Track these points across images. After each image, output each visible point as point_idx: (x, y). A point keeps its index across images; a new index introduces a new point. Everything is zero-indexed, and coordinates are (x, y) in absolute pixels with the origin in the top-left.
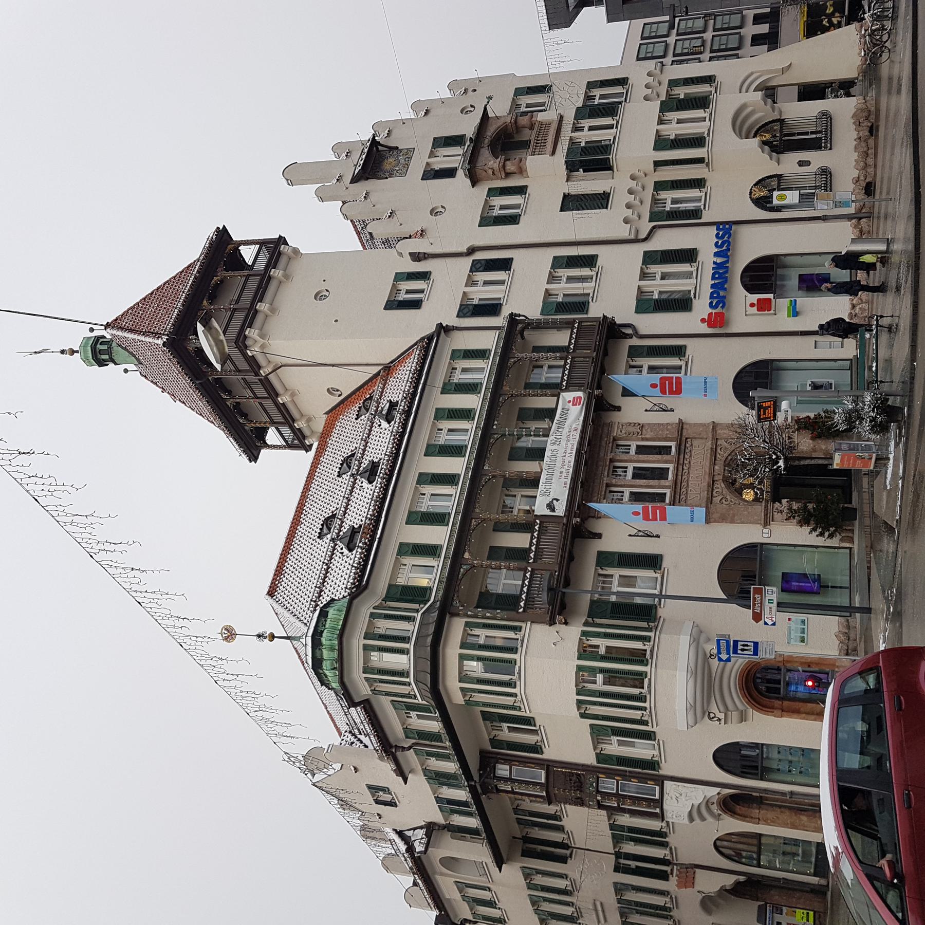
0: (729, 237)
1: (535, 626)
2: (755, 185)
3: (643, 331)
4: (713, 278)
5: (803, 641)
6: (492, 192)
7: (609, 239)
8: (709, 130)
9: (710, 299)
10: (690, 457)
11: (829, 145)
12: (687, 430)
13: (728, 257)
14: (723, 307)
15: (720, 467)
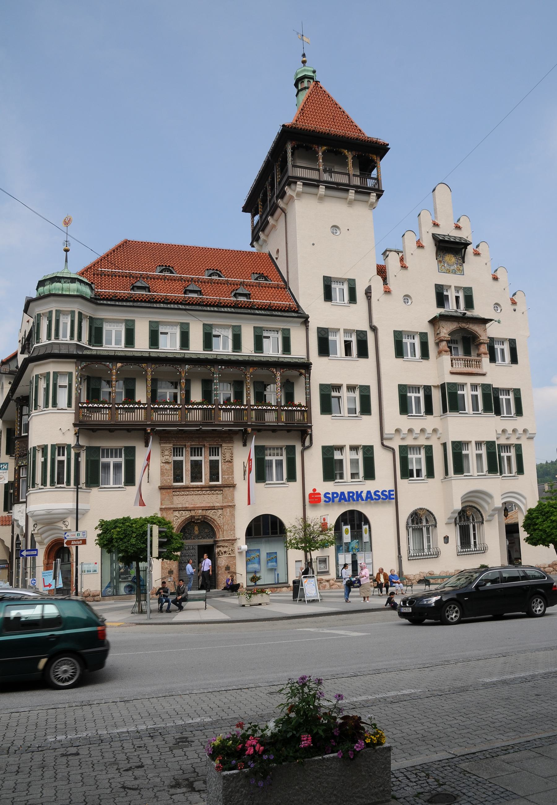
1: (73, 415)
3: (306, 453)
4: (349, 493)
7: (383, 421)
9: (332, 493)
10: (208, 494)
11: (459, 554)
12: (229, 490)
14: (325, 501)
15: (201, 513)
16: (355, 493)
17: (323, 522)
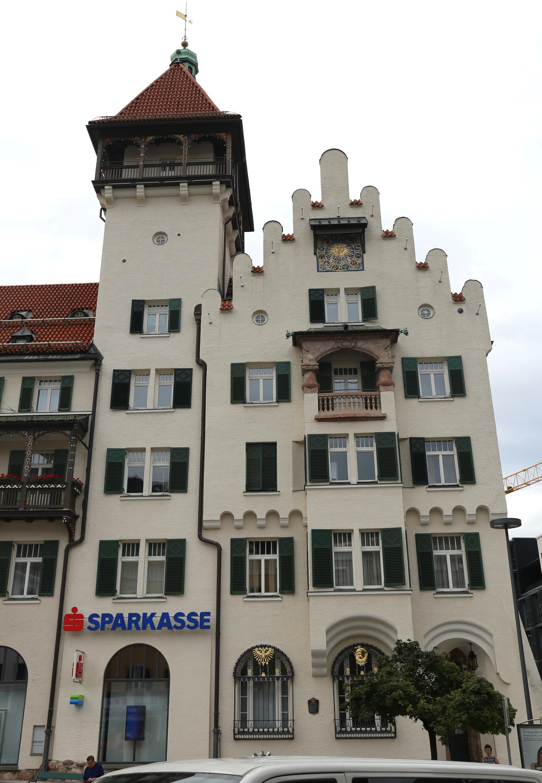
0: (189, 627)
2: (276, 650)
4: (131, 615)
8: (354, 590)
9: (103, 614)
13: (159, 628)
14: (89, 628)
16: (141, 616)
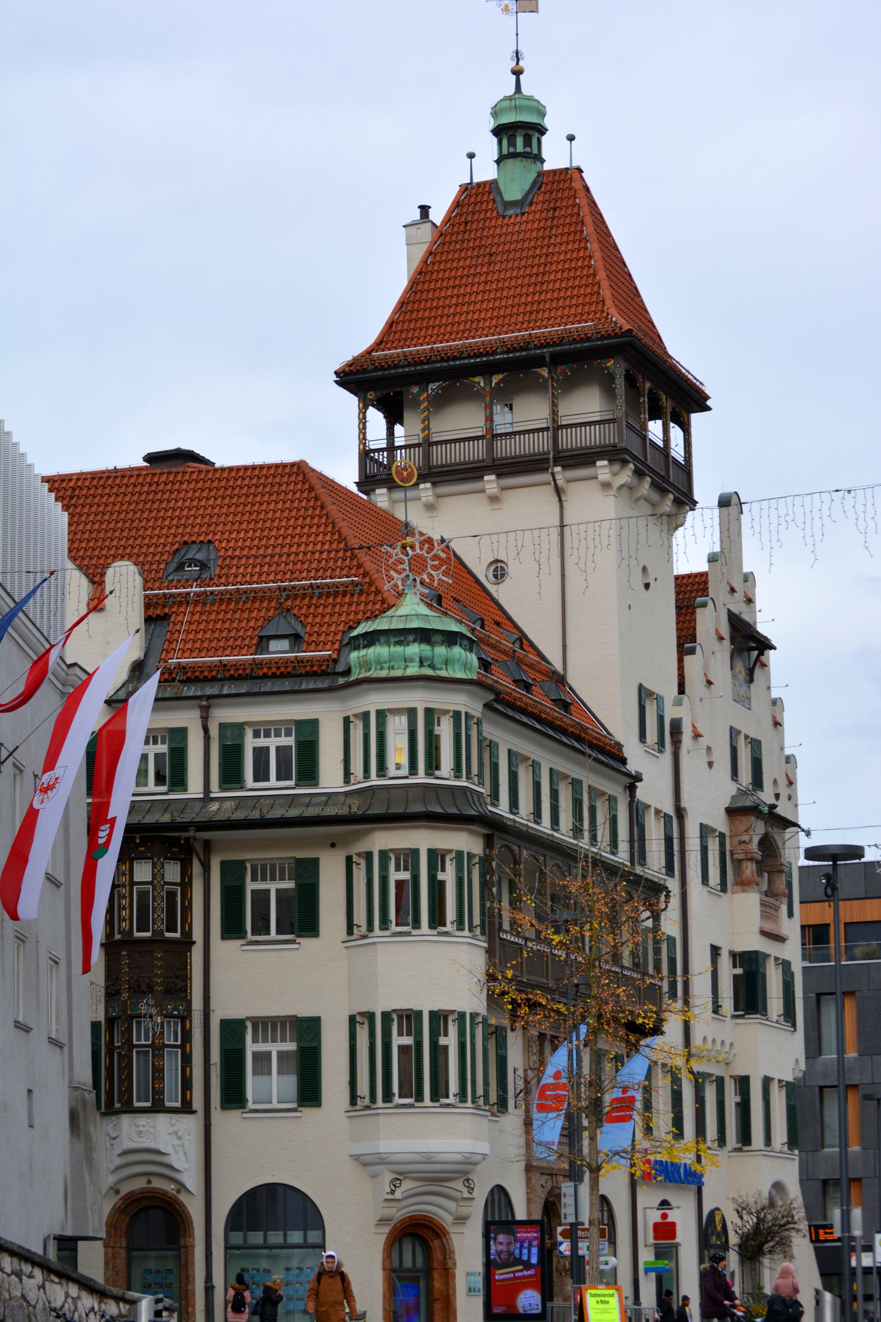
5: (470, 1291)
6: (722, 836)
17: (659, 1220)
